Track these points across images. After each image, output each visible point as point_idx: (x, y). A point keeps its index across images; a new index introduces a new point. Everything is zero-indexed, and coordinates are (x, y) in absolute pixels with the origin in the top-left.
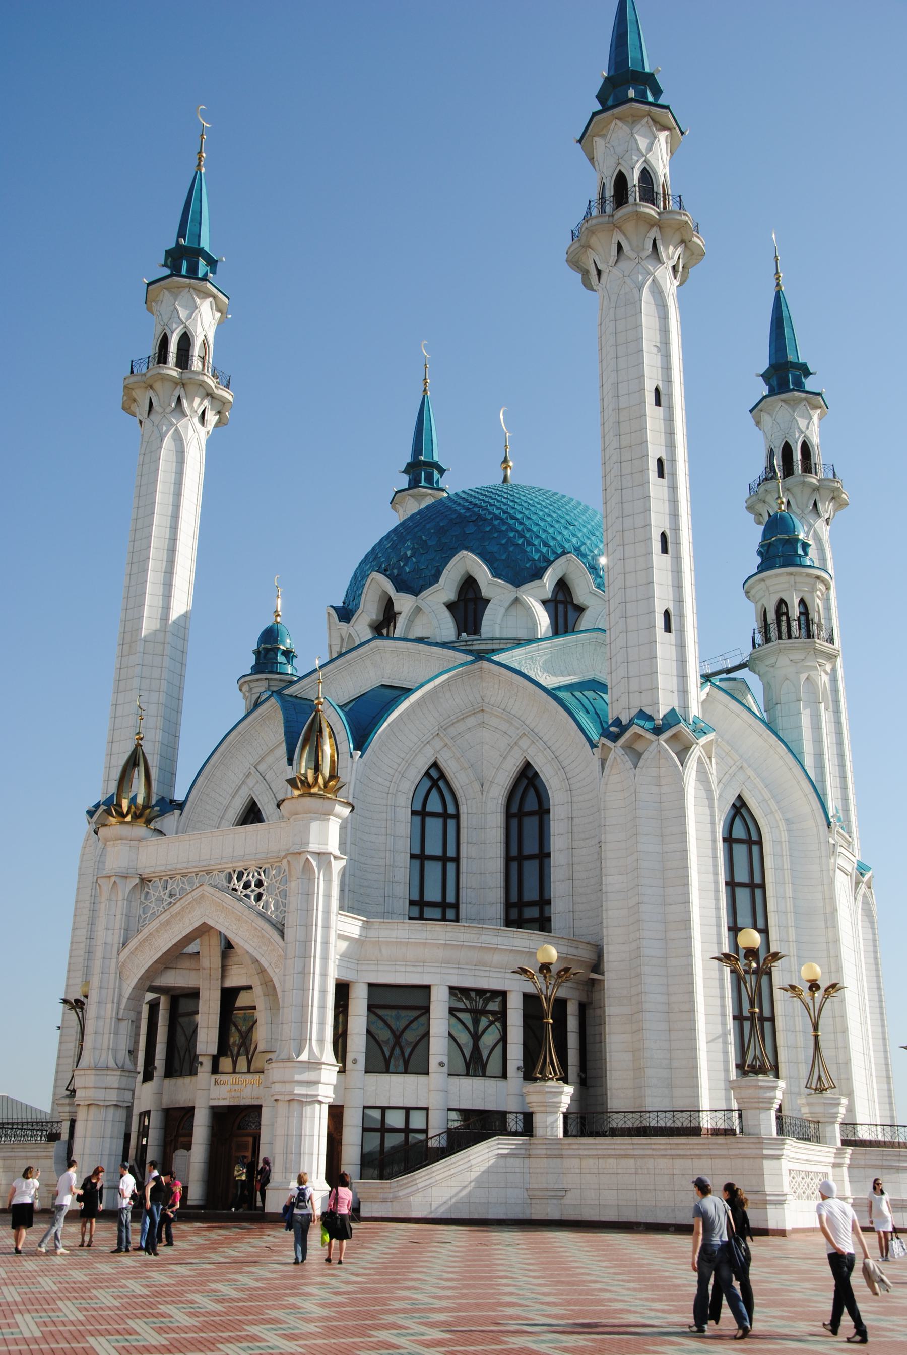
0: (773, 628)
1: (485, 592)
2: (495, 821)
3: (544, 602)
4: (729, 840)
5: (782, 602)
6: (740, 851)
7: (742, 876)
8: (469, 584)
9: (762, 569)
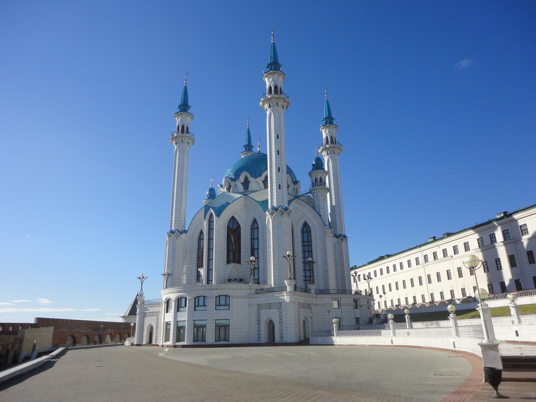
0: (314, 184)
1: (250, 180)
2: (249, 231)
3: (263, 182)
4: (303, 232)
5: (316, 178)
6: (305, 234)
7: (306, 240)
8: (246, 178)
9: (313, 170)
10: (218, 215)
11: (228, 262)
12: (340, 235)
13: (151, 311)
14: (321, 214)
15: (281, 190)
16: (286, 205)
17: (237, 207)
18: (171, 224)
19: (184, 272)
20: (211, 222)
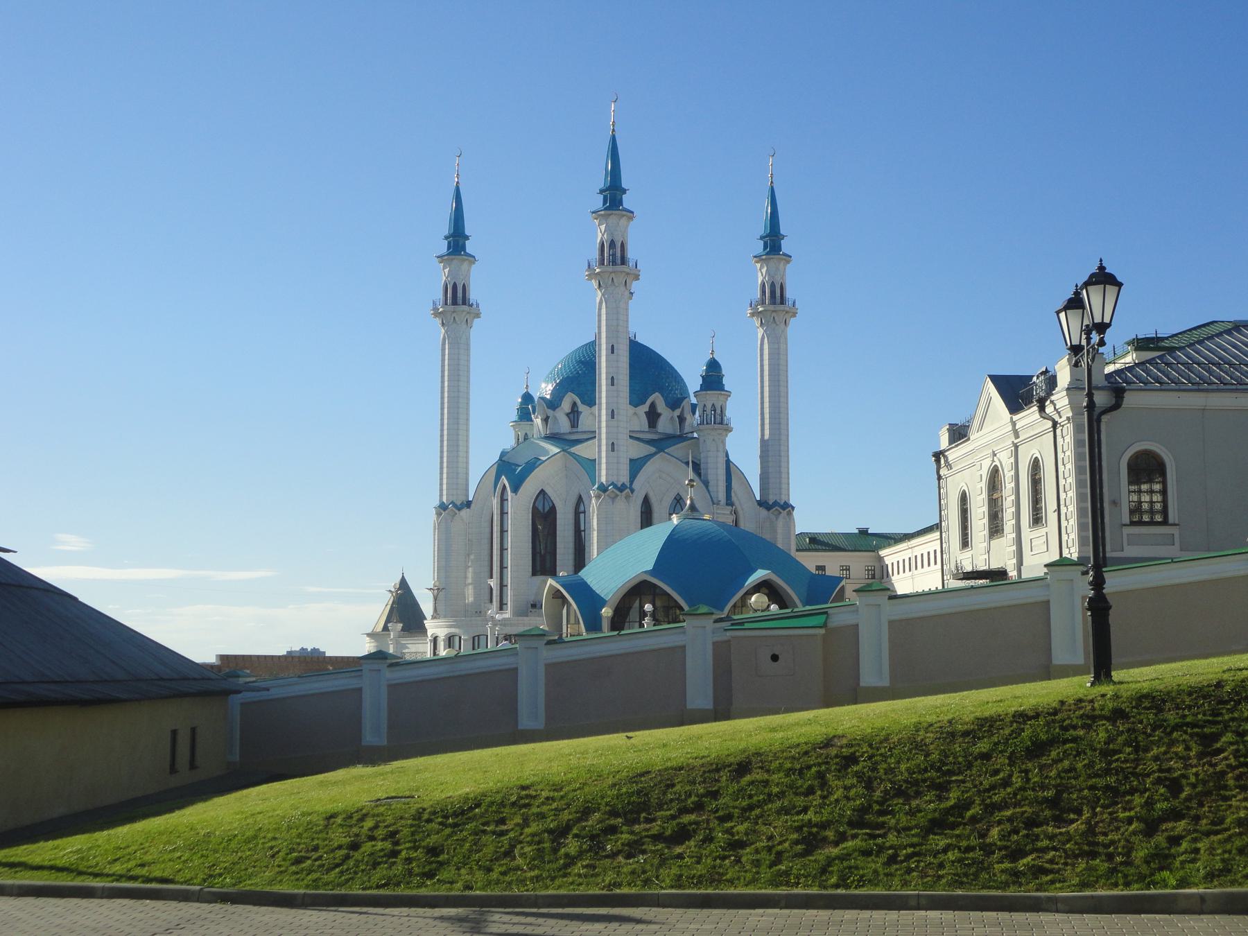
8: (574, 404)
10: (515, 490)
11: (534, 573)
12: (776, 503)
13: (413, 650)
14: (710, 478)
15: (615, 454)
16: (624, 478)
17: (550, 475)
18: (441, 490)
19: (470, 581)
20: (503, 500)
